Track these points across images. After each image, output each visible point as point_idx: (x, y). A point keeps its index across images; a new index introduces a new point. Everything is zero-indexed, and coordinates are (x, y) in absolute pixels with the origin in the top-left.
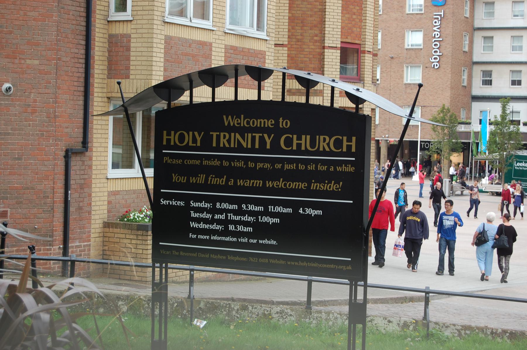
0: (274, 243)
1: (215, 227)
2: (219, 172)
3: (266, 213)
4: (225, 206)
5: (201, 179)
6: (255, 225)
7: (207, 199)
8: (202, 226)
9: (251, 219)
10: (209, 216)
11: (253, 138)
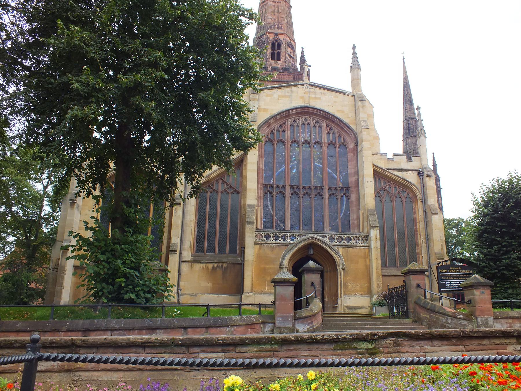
2: (450, 276)
5: (447, 278)
7: (449, 281)
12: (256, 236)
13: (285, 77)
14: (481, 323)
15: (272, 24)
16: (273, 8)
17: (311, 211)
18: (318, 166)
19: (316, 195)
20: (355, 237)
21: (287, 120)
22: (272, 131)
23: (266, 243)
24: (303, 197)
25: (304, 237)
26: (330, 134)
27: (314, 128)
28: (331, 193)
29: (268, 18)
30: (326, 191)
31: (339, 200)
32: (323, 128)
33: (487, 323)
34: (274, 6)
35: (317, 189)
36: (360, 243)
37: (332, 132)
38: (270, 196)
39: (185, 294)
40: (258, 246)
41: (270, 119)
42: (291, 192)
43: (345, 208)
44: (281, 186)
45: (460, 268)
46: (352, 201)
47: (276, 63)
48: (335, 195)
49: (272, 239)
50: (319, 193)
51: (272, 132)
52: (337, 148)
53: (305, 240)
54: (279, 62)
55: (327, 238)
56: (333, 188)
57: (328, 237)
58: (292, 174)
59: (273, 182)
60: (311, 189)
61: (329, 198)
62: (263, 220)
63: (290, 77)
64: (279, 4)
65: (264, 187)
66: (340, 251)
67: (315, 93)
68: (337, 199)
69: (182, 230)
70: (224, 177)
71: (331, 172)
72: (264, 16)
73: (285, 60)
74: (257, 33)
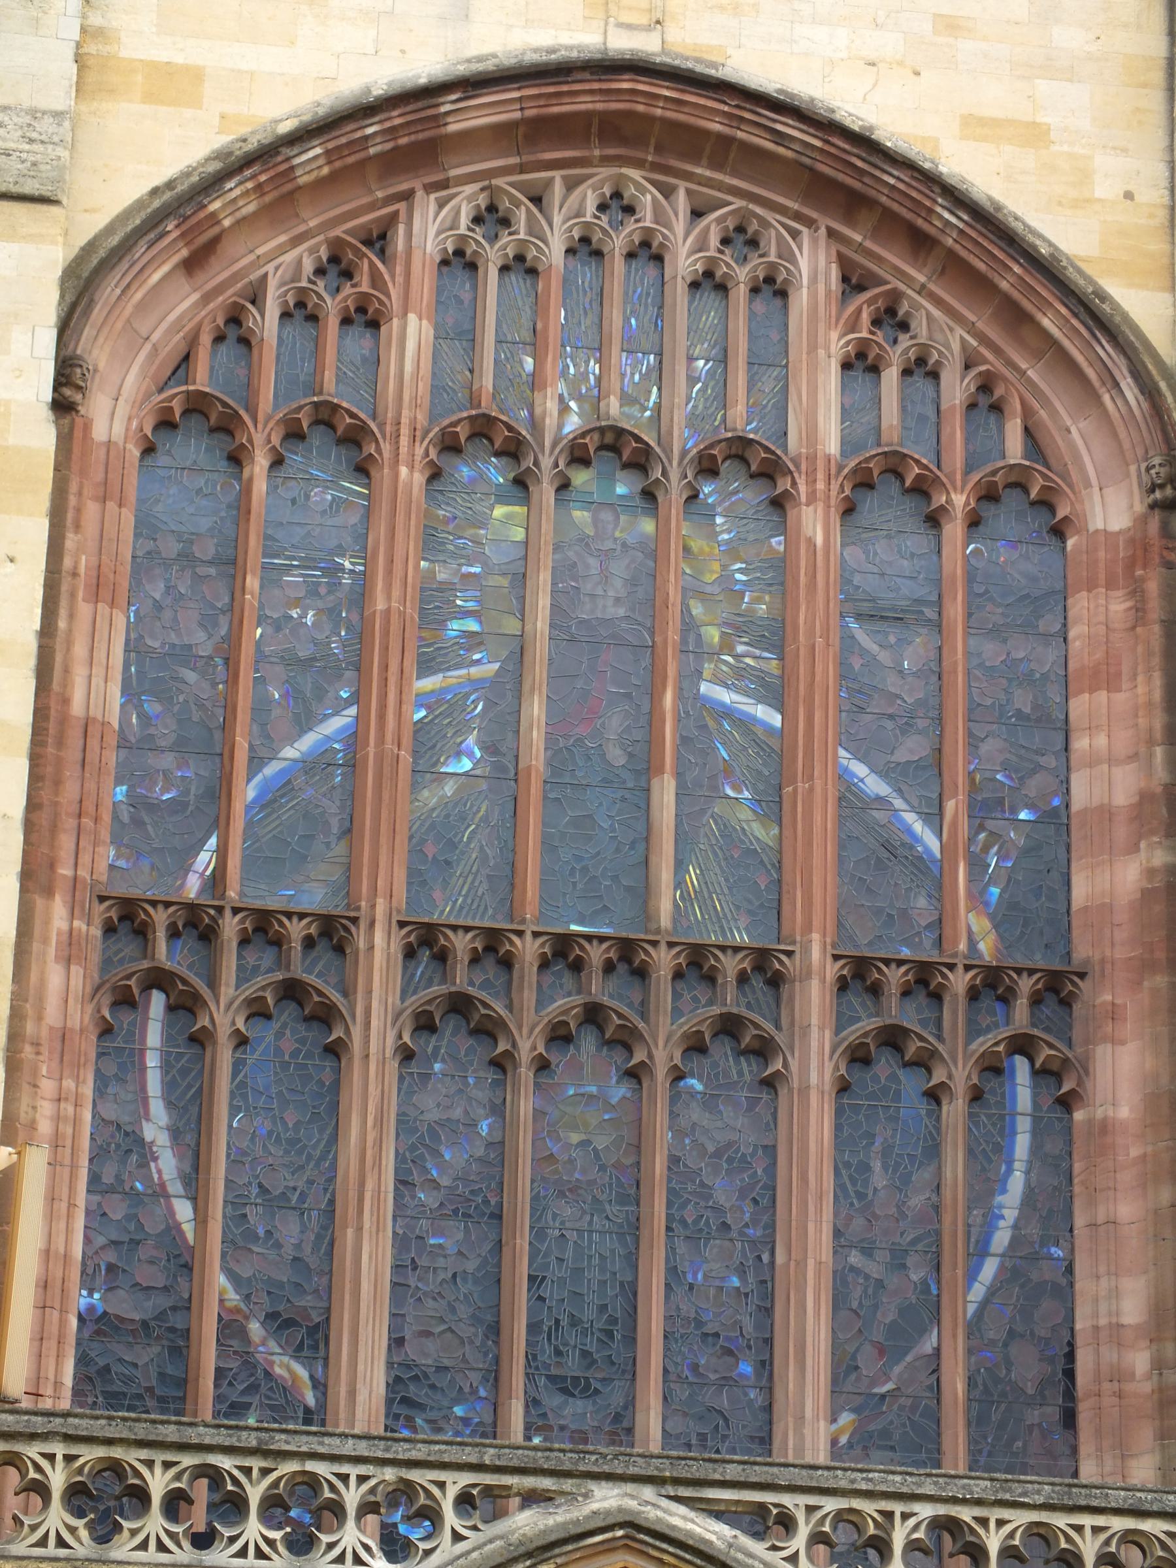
17: (633, 1230)
18: (726, 713)
19: (696, 1047)
21: (408, 196)
22: (235, 319)
24: (543, 1065)
26: (874, 370)
27: (709, 298)
28: (869, 1023)
31: (955, 1109)
32: (801, 299)
35: (710, 978)
37: (896, 356)
38: (168, 1038)
41: (211, 184)
42: (415, 1001)
43: (1029, 1199)
44: (296, 930)
46: (1104, 1128)
48: (912, 1048)
49: (155, 1523)
50: (729, 1026)
52: (954, 529)
55: (799, 1541)
56: (895, 977)
58: (429, 797)
59: (216, 881)
60: (641, 973)
61: (843, 1088)
62: (82, 1300)
65: (109, 929)
68: (934, 1096)
71: (875, 786)
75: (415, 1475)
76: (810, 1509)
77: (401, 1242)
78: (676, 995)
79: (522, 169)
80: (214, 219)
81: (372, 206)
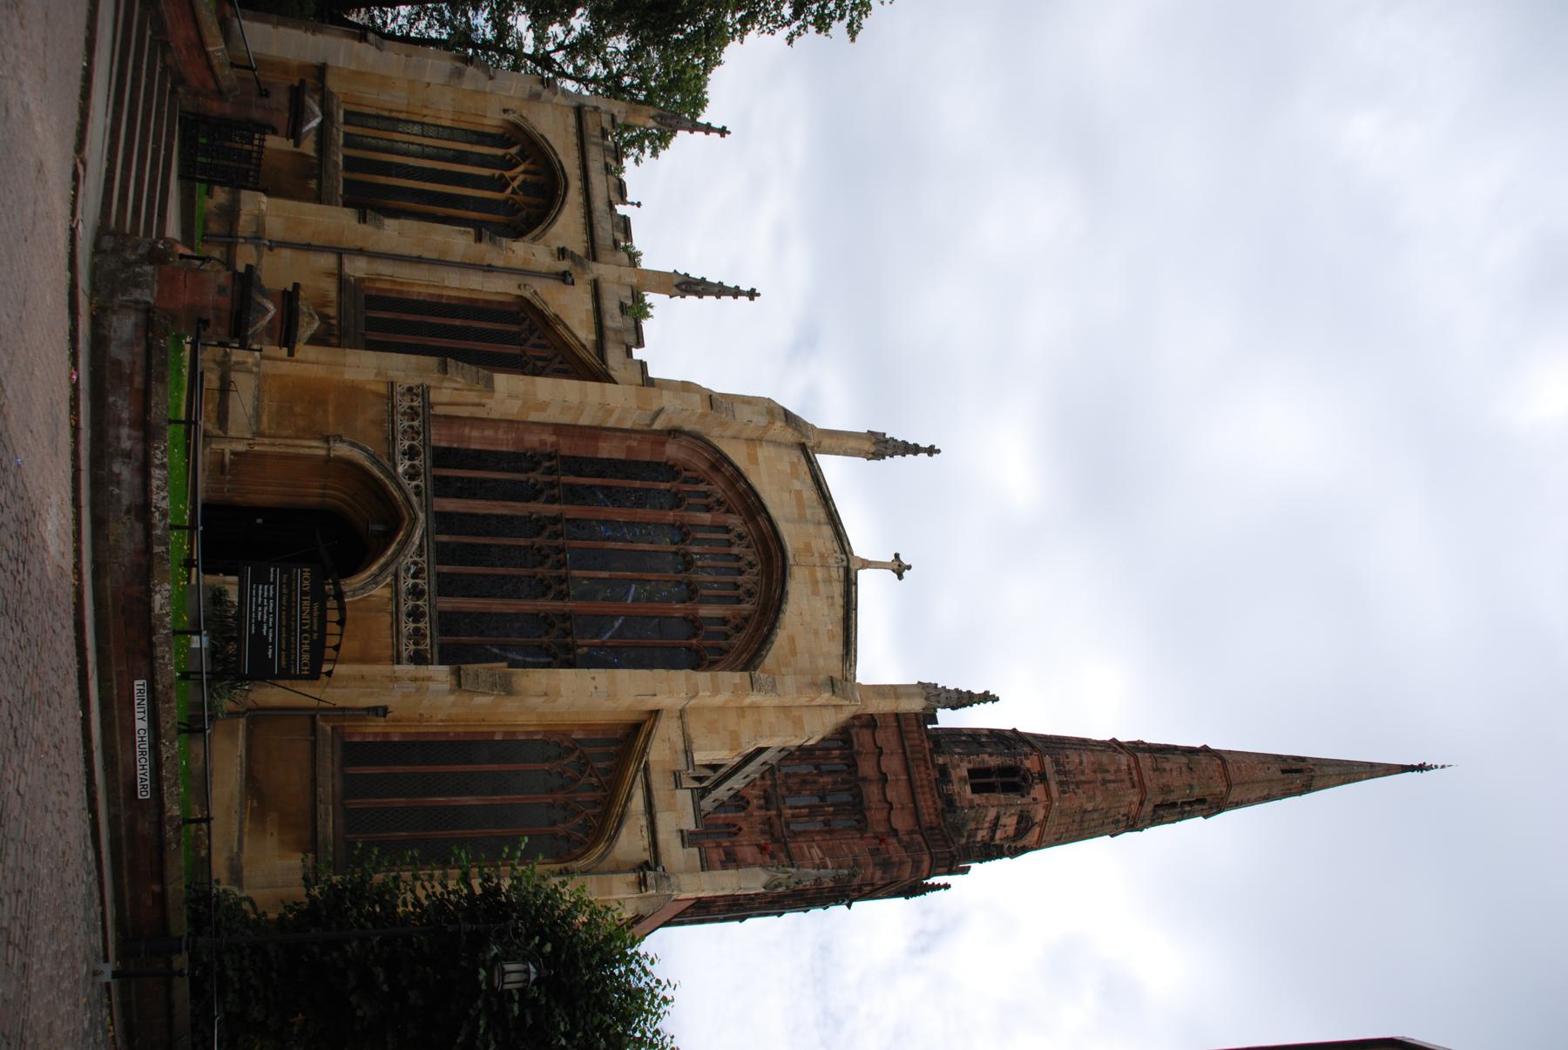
0: (253, 632)
1: (260, 599)
2: (289, 601)
3: (268, 628)
4: (271, 605)
5: (285, 591)
6: (262, 621)
7: (275, 595)
8: (260, 592)
9: (265, 620)
10: (265, 596)
11: (307, 619)
12: (410, 389)
13: (930, 803)
14: (137, 270)
15: (1068, 767)
16: (1112, 768)
18: (629, 590)
20: (424, 636)
21: (741, 515)
23: (393, 407)
25: (414, 499)
29: (1080, 756)
30: (558, 605)
33: (137, 285)
34: (1118, 770)
36: (407, 648)
39: (260, 257)
40: (383, 389)
45: (315, 636)
47: (961, 779)
51: (698, 481)
53: (407, 499)
54: (968, 788)
57: (418, 559)
63: (933, 817)
64: (1128, 784)
66: (381, 592)
67: (828, 581)
69: (419, 260)
70: (561, 362)
71: (617, 625)
72: (1084, 747)
73: (978, 805)
74: (1034, 736)
75: (423, 476)
76: (424, 561)
77: (485, 517)
78: (555, 577)
79: (754, 541)
80: (723, 466)
81: (737, 508)
